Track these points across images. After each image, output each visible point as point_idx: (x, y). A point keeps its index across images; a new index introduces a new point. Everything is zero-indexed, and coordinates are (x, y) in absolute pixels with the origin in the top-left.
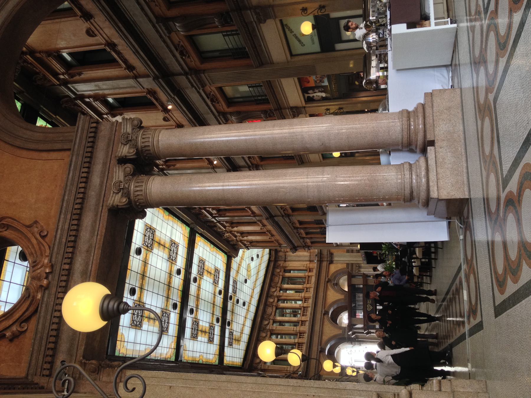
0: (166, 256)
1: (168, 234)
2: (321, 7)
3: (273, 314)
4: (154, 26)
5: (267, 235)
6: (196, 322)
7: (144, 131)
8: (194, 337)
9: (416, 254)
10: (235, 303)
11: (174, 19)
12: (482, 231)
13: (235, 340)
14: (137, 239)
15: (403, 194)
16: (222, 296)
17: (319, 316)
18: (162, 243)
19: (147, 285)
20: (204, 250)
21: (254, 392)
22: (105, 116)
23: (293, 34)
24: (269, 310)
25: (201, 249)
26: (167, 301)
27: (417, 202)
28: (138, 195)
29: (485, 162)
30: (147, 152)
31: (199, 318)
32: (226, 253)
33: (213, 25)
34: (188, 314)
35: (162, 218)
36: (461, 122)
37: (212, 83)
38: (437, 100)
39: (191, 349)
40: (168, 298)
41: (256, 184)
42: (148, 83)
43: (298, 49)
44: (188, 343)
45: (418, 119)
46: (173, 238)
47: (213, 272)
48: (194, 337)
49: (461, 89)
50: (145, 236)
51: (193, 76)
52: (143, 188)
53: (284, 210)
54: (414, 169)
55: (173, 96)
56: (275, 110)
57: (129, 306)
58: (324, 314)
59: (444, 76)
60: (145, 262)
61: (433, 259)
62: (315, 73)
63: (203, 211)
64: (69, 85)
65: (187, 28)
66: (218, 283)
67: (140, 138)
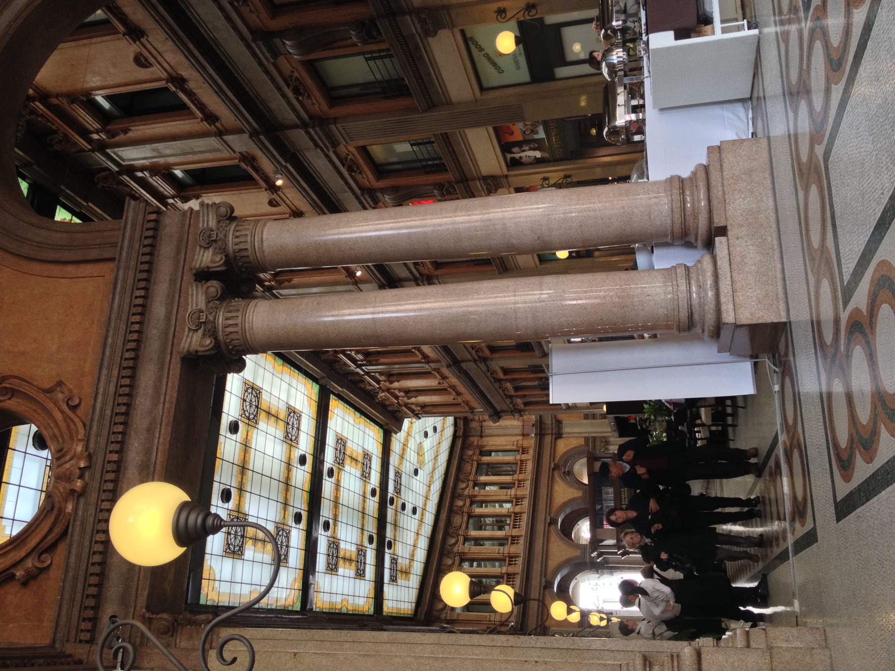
0: (280, 434)
1: (283, 397)
2: (530, 7)
3: (464, 526)
4: (249, 47)
5: (450, 394)
6: (334, 544)
7: (237, 225)
8: (332, 570)
9: (700, 418)
10: (399, 509)
11: (282, 33)
12: (810, 377)
13: (402, 572)
14: (231, 407)
15: (676, 319)
16: (377, 499)
17: (540, 527)
18: (273, 412)
19: (249, 483)
20: (344, 421)
21: (436, 659)
22: (170, 201)
23: (483, 53)
24: (457, 520)
25: (339, 420)
26: (285, 510)
27: (700, 331)
28: (231, 333)
29: (813, 260)
30: (244, 260)
31: (339, 537)
32: (381, 426)
33: (349, 42)
34: (321, 530)
35: (271, 370)
36: (770, 193)
37: (348, 140)
38: (729, 158)
39: (327, 589)
40: (286, 504)
41: (428, 309)
42: (241, 143)
43: (492, 77)
45: (698, 191)
46: (292, 404)
47: (360, 459)
48: (332, 568)
49: (769, 138)
50: (244, 400)
51: (318, 129)
52: (239, 321)
53: (477, 351)
54: (693, 275)
55: (284, 164)
56: (457, 182)
57: (222, 520)
58: (550, 524)
59: (739, 118)
60: (246, 446)
61: (730, 425)
62: (522, 119)
63: (341, 356)
64: (109, 151)
65: (303, 47)
66: (369, 476)
67: (231, 237)
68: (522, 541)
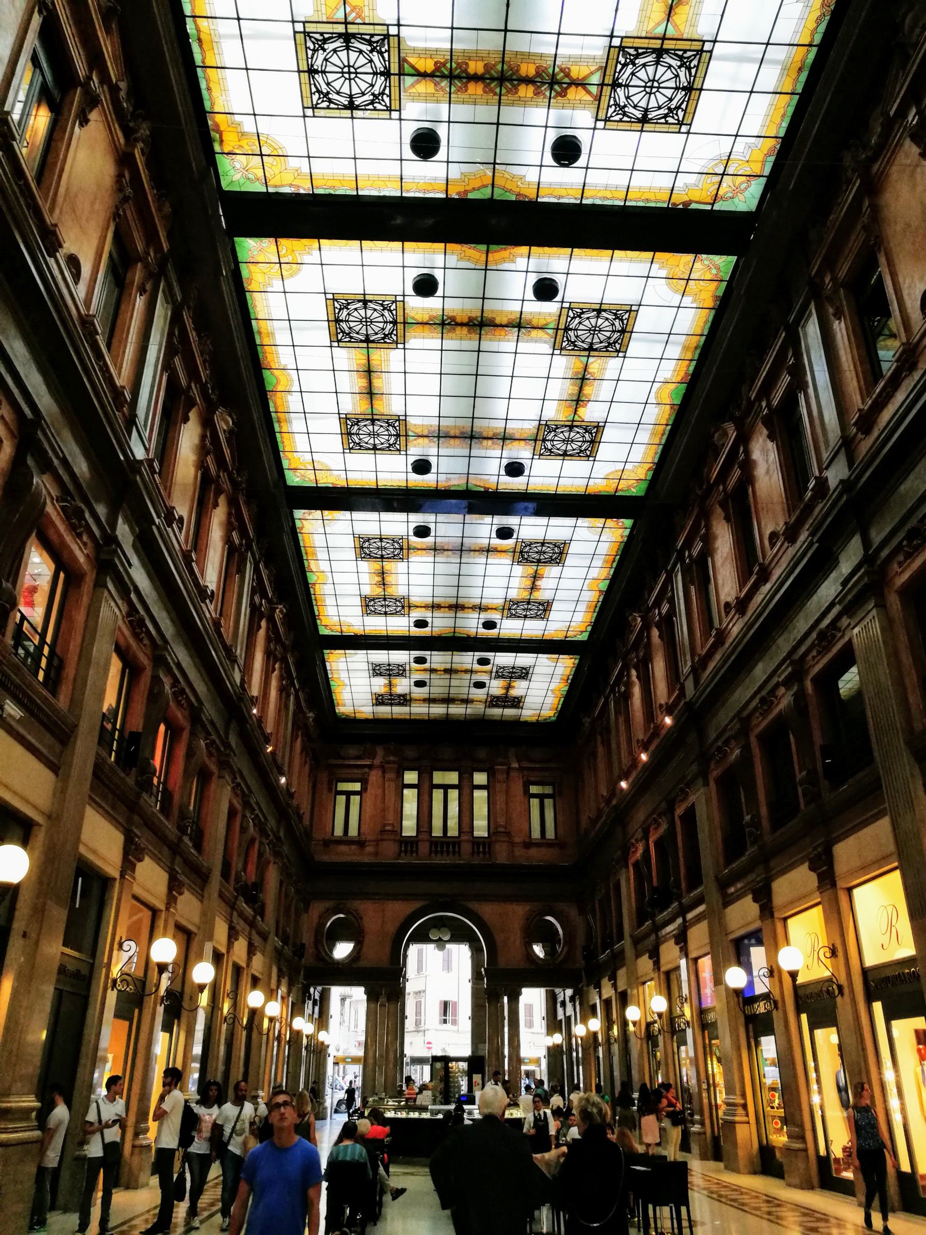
0: (513, 594)
18: (538, 583)
25: (550, 670)
26: (426, 607)
44: (359, 659)
46: (555, 606)
48: (377, 670)
50: (543, 544)
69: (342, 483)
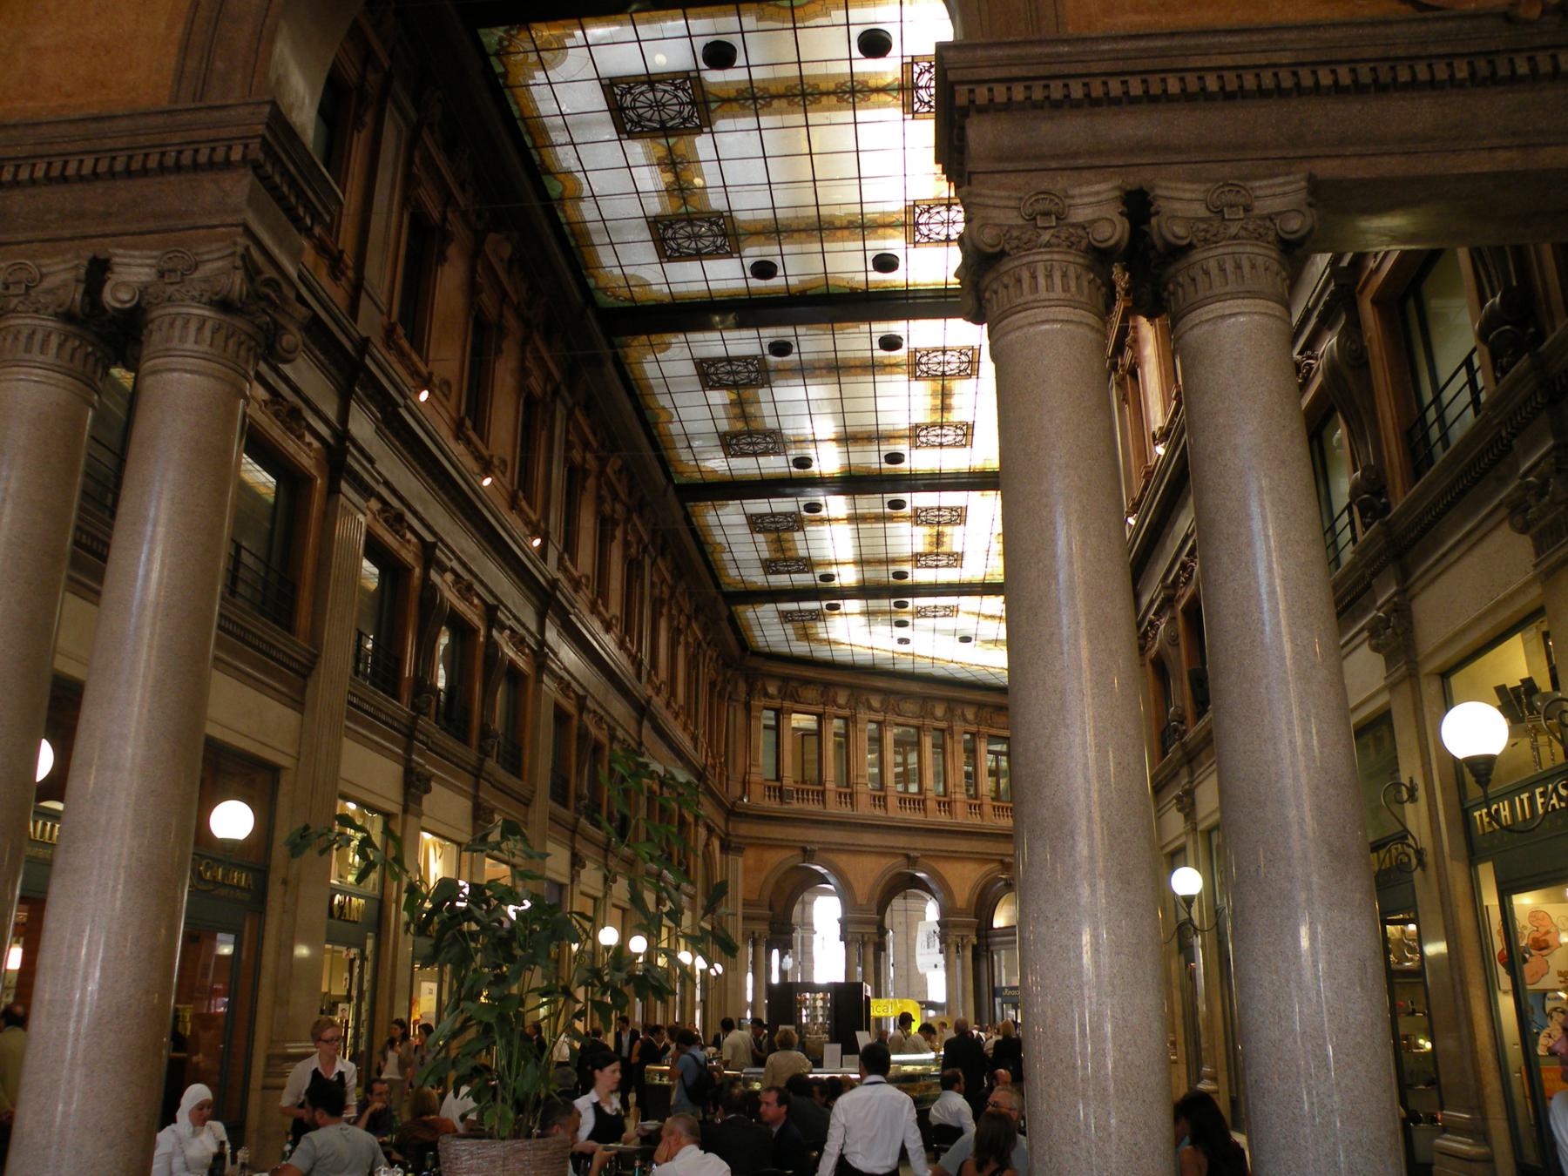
3: (900, 720)
10: (896, 618)
13: (805, 628)
24: (910, 707)
48: (756, 523)
58: (907, 857)
60: (873, 366)
68: (879, 812)
69: (668, 300)
